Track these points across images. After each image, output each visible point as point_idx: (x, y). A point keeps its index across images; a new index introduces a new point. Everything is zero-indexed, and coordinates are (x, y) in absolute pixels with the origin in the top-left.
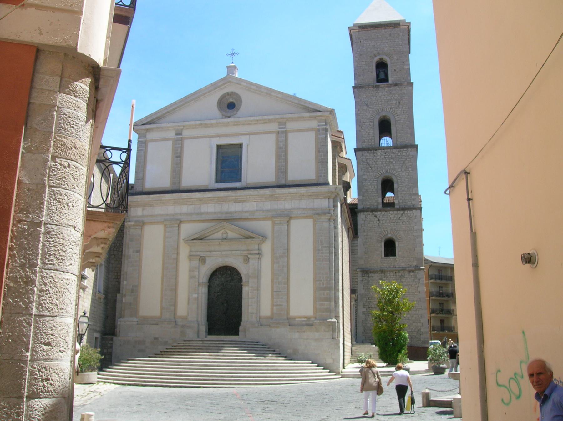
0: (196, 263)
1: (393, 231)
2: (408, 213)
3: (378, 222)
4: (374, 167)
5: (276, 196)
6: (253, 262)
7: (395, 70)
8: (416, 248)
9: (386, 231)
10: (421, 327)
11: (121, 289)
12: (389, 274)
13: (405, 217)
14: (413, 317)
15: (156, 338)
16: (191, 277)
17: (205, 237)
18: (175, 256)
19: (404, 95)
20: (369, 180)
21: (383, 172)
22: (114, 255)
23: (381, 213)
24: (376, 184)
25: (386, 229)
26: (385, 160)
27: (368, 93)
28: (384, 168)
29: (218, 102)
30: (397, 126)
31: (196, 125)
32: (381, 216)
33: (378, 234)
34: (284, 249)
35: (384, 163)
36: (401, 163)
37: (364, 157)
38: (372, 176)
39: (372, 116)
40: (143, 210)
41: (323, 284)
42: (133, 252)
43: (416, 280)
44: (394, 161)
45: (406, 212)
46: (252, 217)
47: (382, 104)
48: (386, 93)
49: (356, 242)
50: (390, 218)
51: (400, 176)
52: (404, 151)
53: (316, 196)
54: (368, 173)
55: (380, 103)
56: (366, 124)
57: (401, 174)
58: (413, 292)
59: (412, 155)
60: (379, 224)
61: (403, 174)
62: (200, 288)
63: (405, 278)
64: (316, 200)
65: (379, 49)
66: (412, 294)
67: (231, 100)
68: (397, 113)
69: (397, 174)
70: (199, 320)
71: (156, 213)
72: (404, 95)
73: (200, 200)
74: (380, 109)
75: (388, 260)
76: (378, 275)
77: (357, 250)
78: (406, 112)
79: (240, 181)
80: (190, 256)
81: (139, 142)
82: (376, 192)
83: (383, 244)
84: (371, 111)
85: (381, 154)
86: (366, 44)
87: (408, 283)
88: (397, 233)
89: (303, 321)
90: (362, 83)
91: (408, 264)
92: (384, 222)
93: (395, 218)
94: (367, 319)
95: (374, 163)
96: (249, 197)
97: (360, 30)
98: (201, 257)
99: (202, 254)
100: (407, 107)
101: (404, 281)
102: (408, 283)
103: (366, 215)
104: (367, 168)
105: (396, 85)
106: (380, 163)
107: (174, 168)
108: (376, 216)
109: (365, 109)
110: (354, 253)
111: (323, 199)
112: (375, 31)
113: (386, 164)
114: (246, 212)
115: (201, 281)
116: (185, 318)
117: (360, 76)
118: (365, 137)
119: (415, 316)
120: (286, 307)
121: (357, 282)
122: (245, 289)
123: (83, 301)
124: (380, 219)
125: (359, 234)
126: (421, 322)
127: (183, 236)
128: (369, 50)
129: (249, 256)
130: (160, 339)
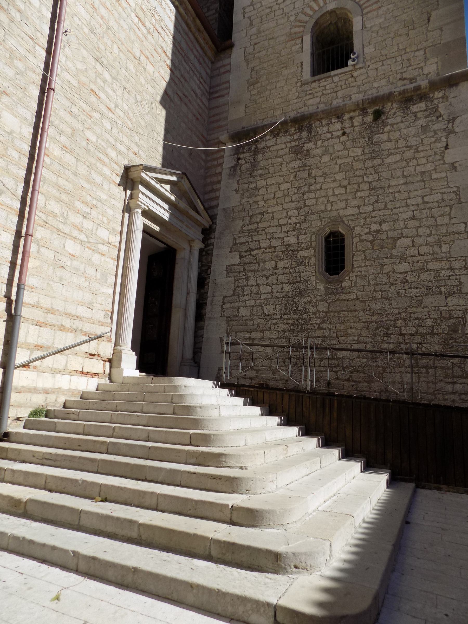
12: (325, 129)
14: (424, 269)
33: (292, 18)
43: (435, 127)
49: (226, 62)
58: (423, 173)
63: (387, 128)
66: (419, 178)
75: (323, 83)
76: (288, 139)
83: (307, 40)
87: (401, 143)
91: (402, 79)
94: (239, 291)
101: (384, 137)
110: (216, 95)
119: (432, 266)
125: (235, 36)
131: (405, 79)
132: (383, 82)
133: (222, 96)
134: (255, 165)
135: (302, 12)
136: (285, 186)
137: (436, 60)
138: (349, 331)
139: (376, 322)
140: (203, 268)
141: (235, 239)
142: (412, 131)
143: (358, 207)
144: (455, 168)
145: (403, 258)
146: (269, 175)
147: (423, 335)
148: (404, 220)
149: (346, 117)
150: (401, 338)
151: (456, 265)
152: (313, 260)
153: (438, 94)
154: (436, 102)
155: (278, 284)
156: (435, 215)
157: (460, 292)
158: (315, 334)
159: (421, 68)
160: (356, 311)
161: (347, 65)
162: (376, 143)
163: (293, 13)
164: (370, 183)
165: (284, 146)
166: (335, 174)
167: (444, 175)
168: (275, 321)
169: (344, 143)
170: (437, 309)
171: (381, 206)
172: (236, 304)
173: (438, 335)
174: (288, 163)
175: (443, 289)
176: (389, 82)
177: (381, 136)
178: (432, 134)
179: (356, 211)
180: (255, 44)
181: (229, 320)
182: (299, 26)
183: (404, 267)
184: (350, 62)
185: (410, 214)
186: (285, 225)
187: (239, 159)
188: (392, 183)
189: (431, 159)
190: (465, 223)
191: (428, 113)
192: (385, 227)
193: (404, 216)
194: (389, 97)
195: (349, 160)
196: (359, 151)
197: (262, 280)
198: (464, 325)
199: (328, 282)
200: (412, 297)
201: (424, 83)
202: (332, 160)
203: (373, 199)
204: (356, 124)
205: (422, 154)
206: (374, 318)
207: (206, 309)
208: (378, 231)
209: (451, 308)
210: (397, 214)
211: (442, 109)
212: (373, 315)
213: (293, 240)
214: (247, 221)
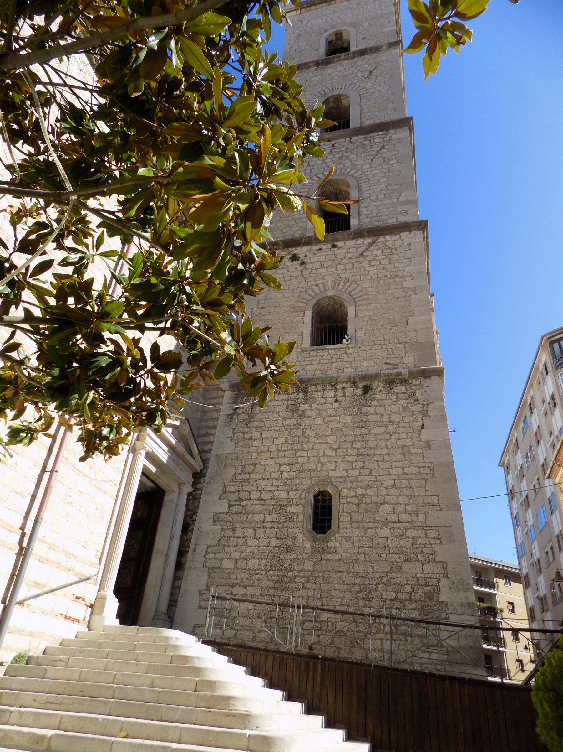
1: (342, 283)
2: (386, 241)
3: (299, 268)
7: (364, 38)
8: (411, 319)
9: (321, 285)
10: (439, 580)
12: (320, 394)
13: (378, 249)
14: (403, 536)
19: (381, 63)
25: (320, 281)
26: (331, 156)
28: (327, 168)
30: (362, 104)
33: (297, 295)
36: (368, 155)
43: (413, 408)
44: (352, 154)
45: (382, 239)
48: (343, 68)
50: (336, 256)
51: (366, 175)
52: (378, 135)
57: (368, 173)
58: (403, 447)
59: (398, 139)
61: (373, 172)
63: (374, 403)
66: (400, 451)
68: (364, 88)
69: (360, 173)
72: (381, 63)
74: (329, 89)
75: (320, 353)
76: (285, 397)
78: (385, 83)
83: (309, 315)
87: (385, 418)
88: (354, 285)
92: (317, 265)
93: (349, 255)
97: (303, 10)
100: (389, 76)
101: (371, 410)
102: (385, 418)
105: (362, 53)
108: (294, 258)
112: (330, 7)
119: (411, 533)
124: (306, 260)
126: (439, 559)
128: (315, 28)
131: (389, 364)
132: (372, 363)
134: (251, 416)
135: (305, 292)
136: (279, 441)
137: (413, 354)
138: (333, 593)
139: (359, 585)
140: (189, 513)
141: (225, 487)
142: (395, 408)
143: (347, 470)
144: (429, 446)
145: (385, 523)
146: (265, 429)
147: (402, 601)
148: (387, 487)
149: (339, 386)
150: (381, 603)
151: (431, 534)
152: (301, 517)
153: (415, 382)
154: (413, 387)
155: (266, 538)
156: (414, 486)
157: (434, 561)
158: (300, 593)
159: (402, 358)
160: (340, 572)
161: (342, 343)
162: (364, 414)
163: (298, 291)
164: (357, 449)
165: (281, 403)
166: (327, 436)
167: (420, 451)
168: (259, 577)
169: (336, 410)
170: (415, 575)
171: (367, 472)
172: (220, 556)
173: (416, 601)
174: (284, 420)
175: (419, 556)
176: (376, 363)
177: (369, 408)
178: (411, 414)
179: (344, 474)
180: (262, 308)
181: (211, 571)
182: (302, 302)
183: (385, 532)
184: (344, 341)
185: (392, 482)
186: (276, 479)
188: (377, 452)
189: (410, 435)
190: (438, 496)
191: (407, 395)
192: (369, 492)
193: (387, 484)
194: (376, 376)
195: (340, 426)
196: (349, 419)
197: (249, 533)
198: (438, 593)
199: (315, 541)
200: (392, 562)
201: (404, 371)
202: (324, 423)
203: (360, 464)
204: (347, 394)
205: (402, 430)
206: (357, 581)
207: (187, 558)
208: (363, 495)
209: (427, 575)
210: (381, 481)
211: (418, 395)
212: (356, 577)
213: (283, 495)
214: (239, 470)
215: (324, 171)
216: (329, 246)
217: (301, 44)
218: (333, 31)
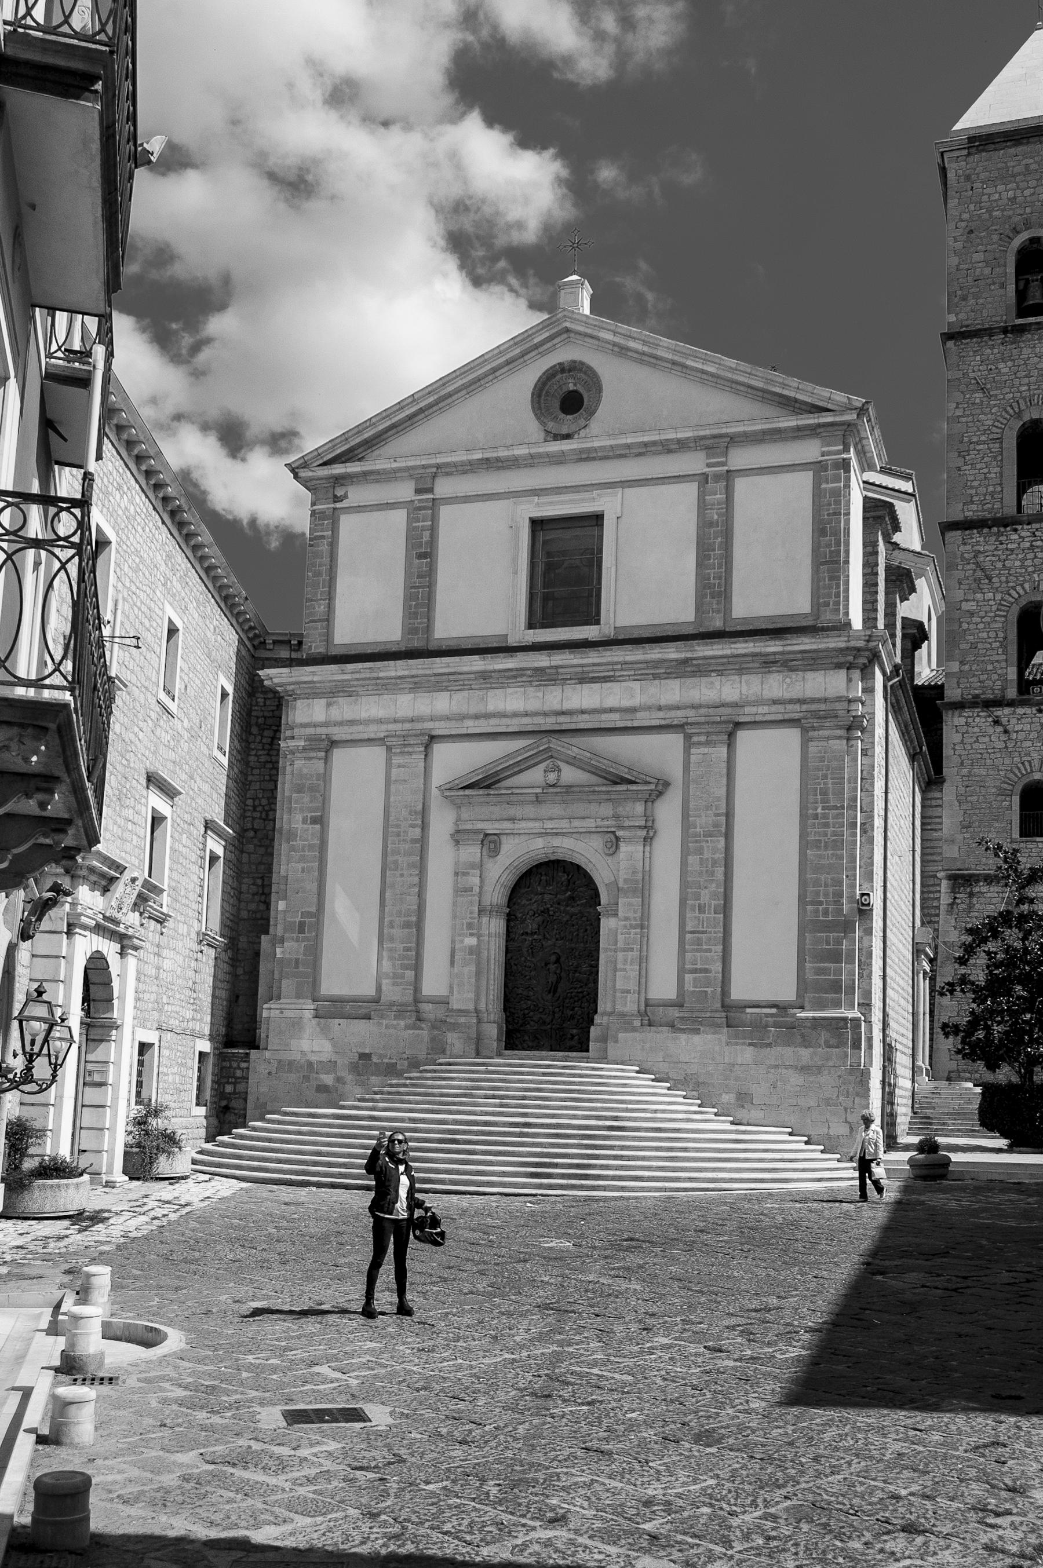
0: (472, 852)
3: (1003, 737)
4: (999, 575)
5: (694, 662)
6: (630, 851)
11: (272, 921)
15: (365, 1057)
16: (461, 891)
17: (499, 781)
18: (418, 831)
20: (982, 614)
21: (1023, 588)
22: (253, 829)
23: (1014, 713)
24: (1000, 625)
26: (1032, 555)
27: (989, 351)
28: (1027, 578)
29: (533, 394)
31: (470, 463)
32: (1014, 721)
34: (717, 815)
35: (1028, 563)
37: (968, 547)
38: (991, 603)
39: (996, 424)
40: (329, 705)
41: (826, 913)
42: (304, 821)
46: (629, 724)
47: (1028, 385)
49: (937, 795)
53: (813, 662)
54: (979, 596)
55: (1026, 380)
56: (978, 447)
60: (1005, 741)
62: (485, 920)
64: (810, 675)
65: (1028, 210)
67: (571, 387)
70: (482, 1006)
71: (364, 715)
73: (485, 676)
74: (1024, 399)
77: (941, 817)
79: (598, 622)
80: (458, 831)
81: (313, 513)
82: (1000, 650)
84: (995, 406)
85: (1020, 537)
86: (989, 195)
89: (767, 1015)
90: (969, 322)
92: (1021, 736)
95: (999, 565)
96: (619, 666)
97: (973, 150)
98: (486, 835)
99: (491, 828)
103: (967, 718)
104: (978, 581)
106: (1018, 563)
107: (412, 588)
108: (997, 722)
109: (978, 401)
111: (832, 672)
113: (1034, 566)
114: (611, 710)
115: (487, 900)
116: (443, 1002)
117: (964, 298)
118: (972, 487)
120: (720, 975)
121: (938, 907)
122: (607, 925)
123: (159, 955)
127: (439, 776)
128: (995, 213)
129: (619, 833)
130: (375, 1059)
133: (935, 830)
187: (955, 898)
215: (1025, 581)
216: (1034, 710)
217: (977, 257)
218: (1024, 236)
